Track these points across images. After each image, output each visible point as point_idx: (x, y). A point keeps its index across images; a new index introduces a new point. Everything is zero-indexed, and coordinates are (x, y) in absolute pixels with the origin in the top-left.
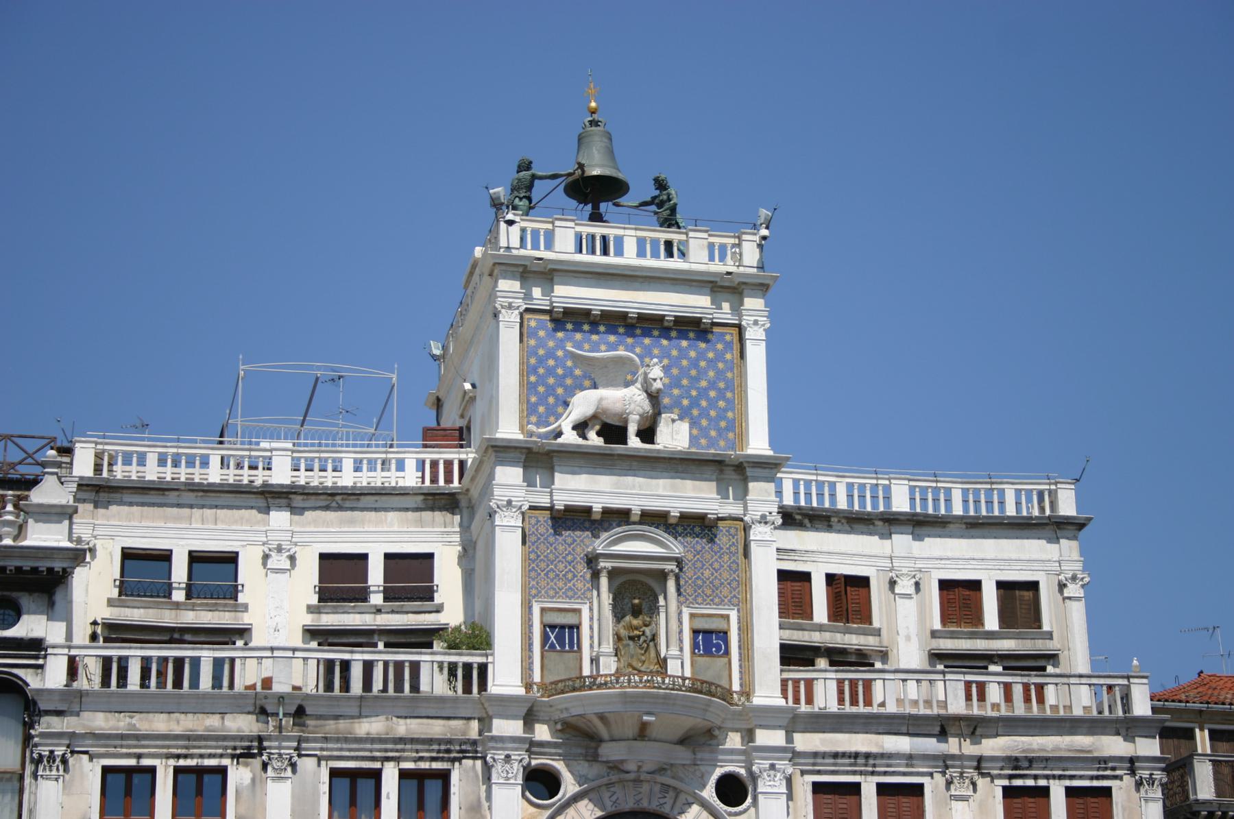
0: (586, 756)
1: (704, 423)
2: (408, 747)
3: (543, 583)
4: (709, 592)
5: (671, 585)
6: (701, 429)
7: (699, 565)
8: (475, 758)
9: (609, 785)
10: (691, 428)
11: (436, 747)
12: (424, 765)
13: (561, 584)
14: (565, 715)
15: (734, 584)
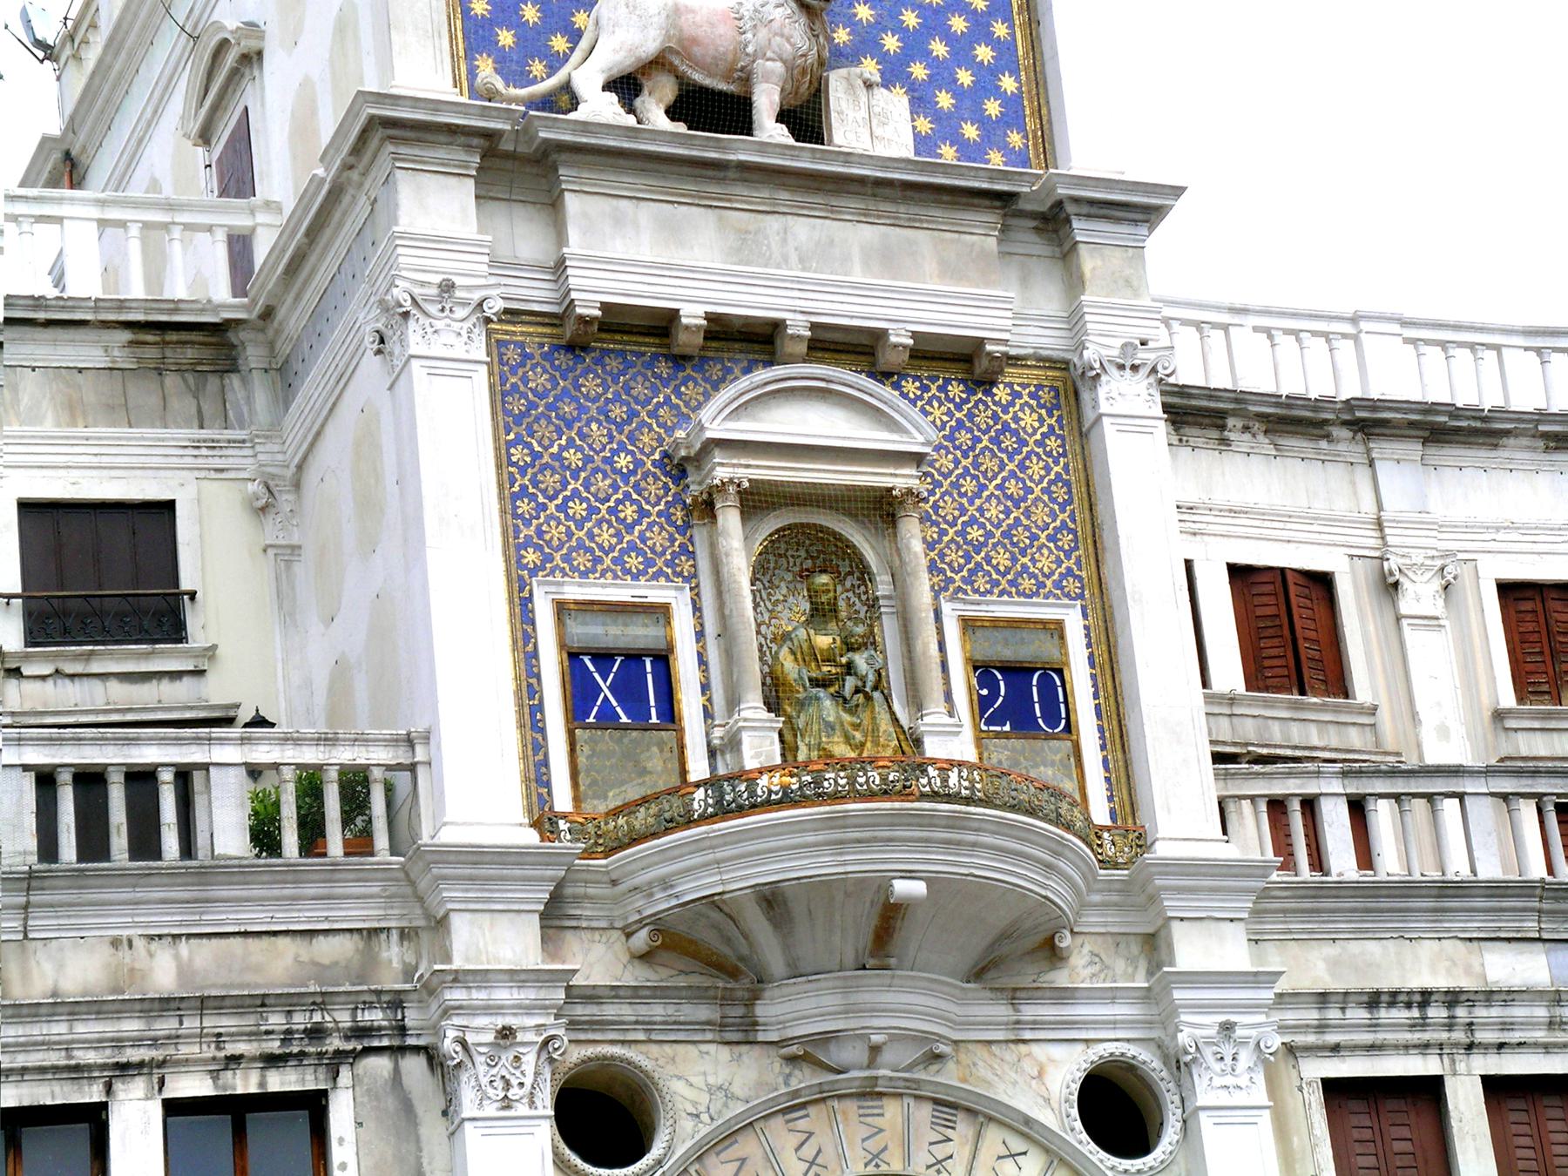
0: (723, 1026)
1: (945, 100)
2: (192, 1024)
3: (555, 533)
4: (1002, 559)
5: (913, 534)
6: (937, 116)
7: (969, 486)
8: (402, 1050)
9: (793, 1107)
10: (914, 113)
11: (276, 1020)
12: (245, 1083)
13: (606, 536)
14: (661, 903)
15: (1066, 540)
